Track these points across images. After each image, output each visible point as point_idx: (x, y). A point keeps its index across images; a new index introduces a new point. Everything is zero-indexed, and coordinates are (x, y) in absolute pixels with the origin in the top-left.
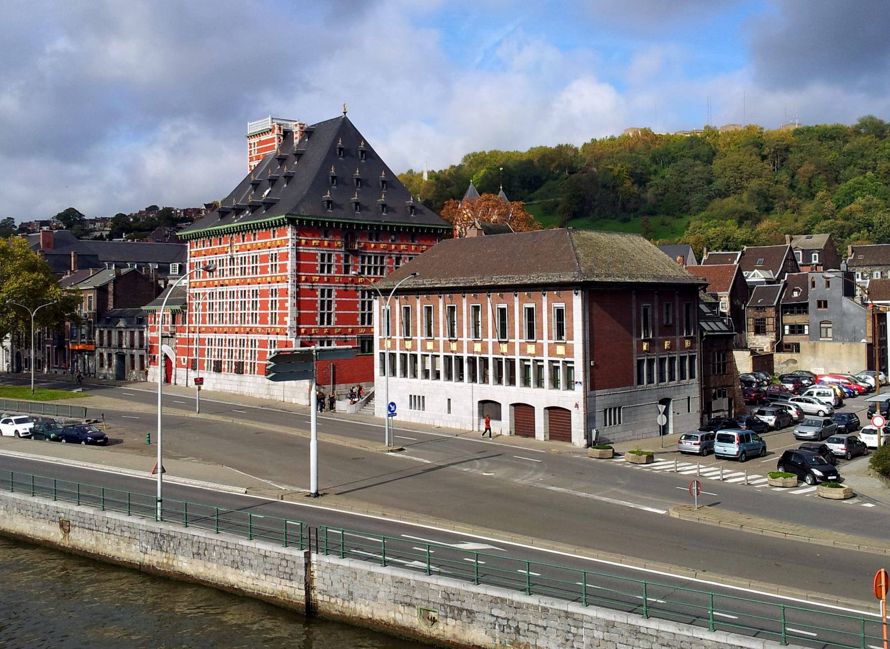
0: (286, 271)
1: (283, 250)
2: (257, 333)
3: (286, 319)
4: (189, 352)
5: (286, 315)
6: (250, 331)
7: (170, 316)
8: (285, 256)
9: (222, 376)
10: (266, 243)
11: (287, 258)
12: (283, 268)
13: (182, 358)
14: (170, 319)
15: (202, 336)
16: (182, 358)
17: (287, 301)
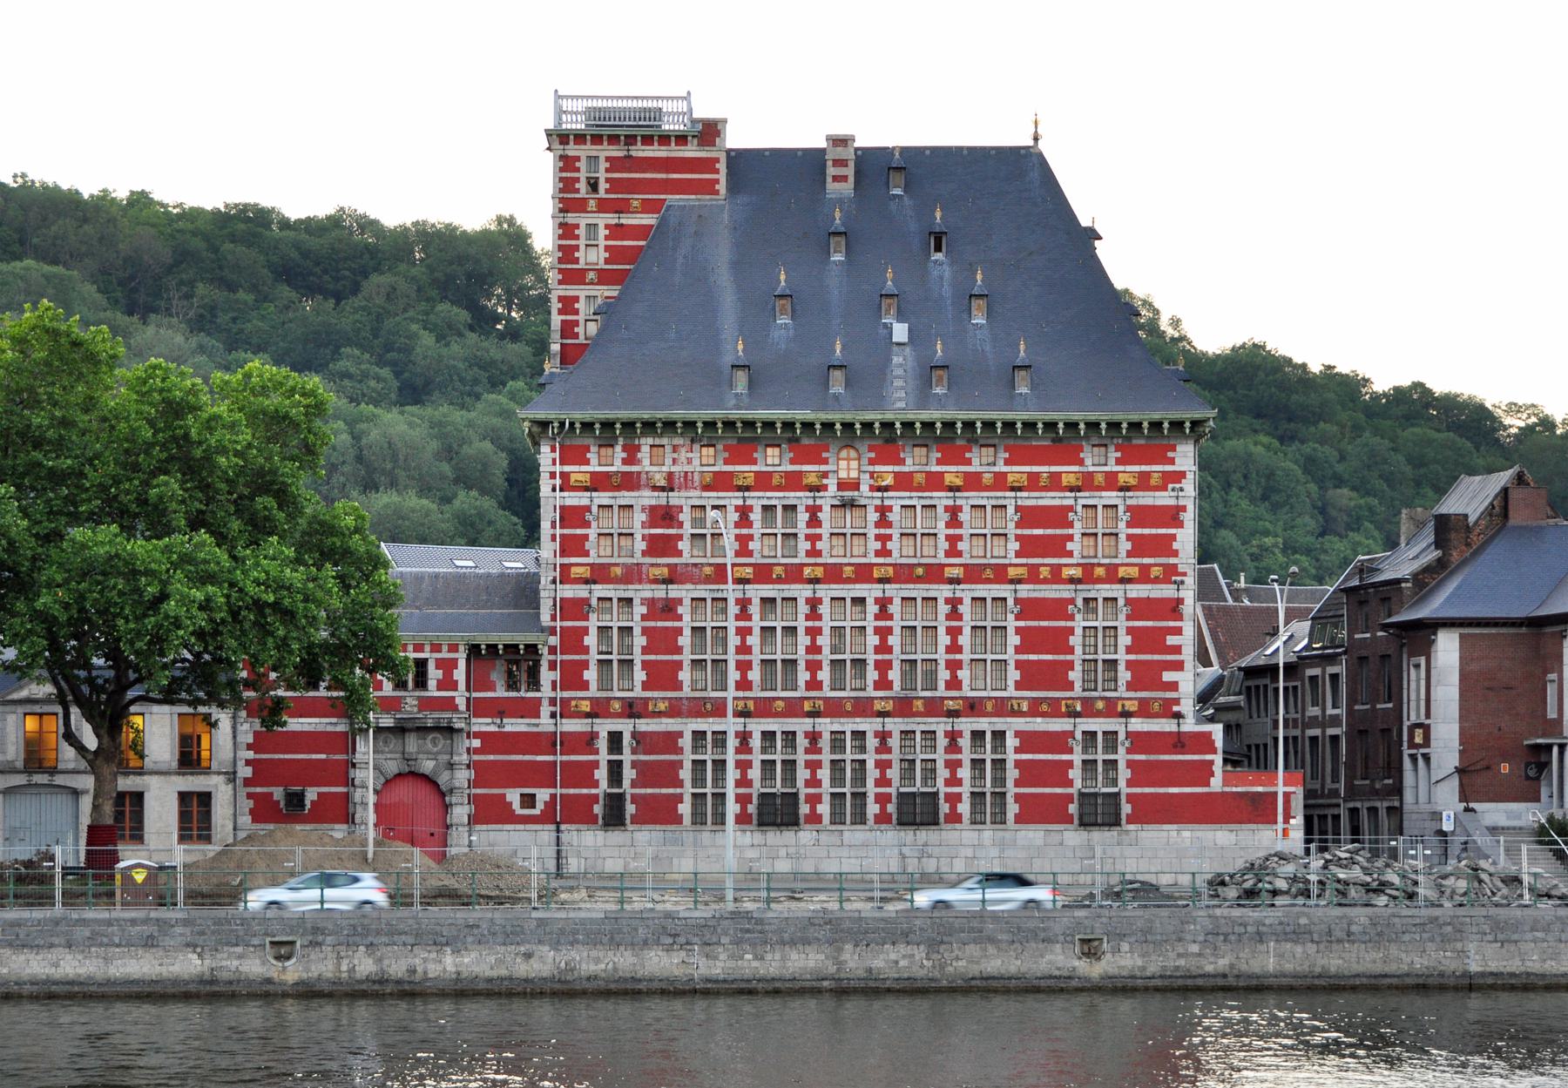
0: (1175, 554)
1: (1163, 499)
2: (1018, 713)
3: (1168, 676)
4: (584, 775)
5: (1179, 666)
6: (973, 707)
7: (462, 664)
8: (1172, 516)
9: (806, 835)
10: (1055, 477)
11: (1180, 525)
12: (1164, 546)
13: (513, 796)
14: (460, 674)
15: (645, 725)
16: (513, 796)
17: (1178, 631)
